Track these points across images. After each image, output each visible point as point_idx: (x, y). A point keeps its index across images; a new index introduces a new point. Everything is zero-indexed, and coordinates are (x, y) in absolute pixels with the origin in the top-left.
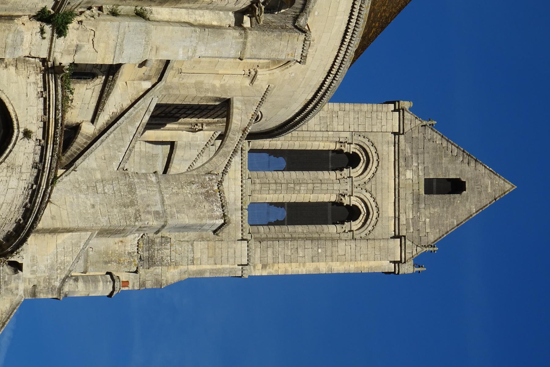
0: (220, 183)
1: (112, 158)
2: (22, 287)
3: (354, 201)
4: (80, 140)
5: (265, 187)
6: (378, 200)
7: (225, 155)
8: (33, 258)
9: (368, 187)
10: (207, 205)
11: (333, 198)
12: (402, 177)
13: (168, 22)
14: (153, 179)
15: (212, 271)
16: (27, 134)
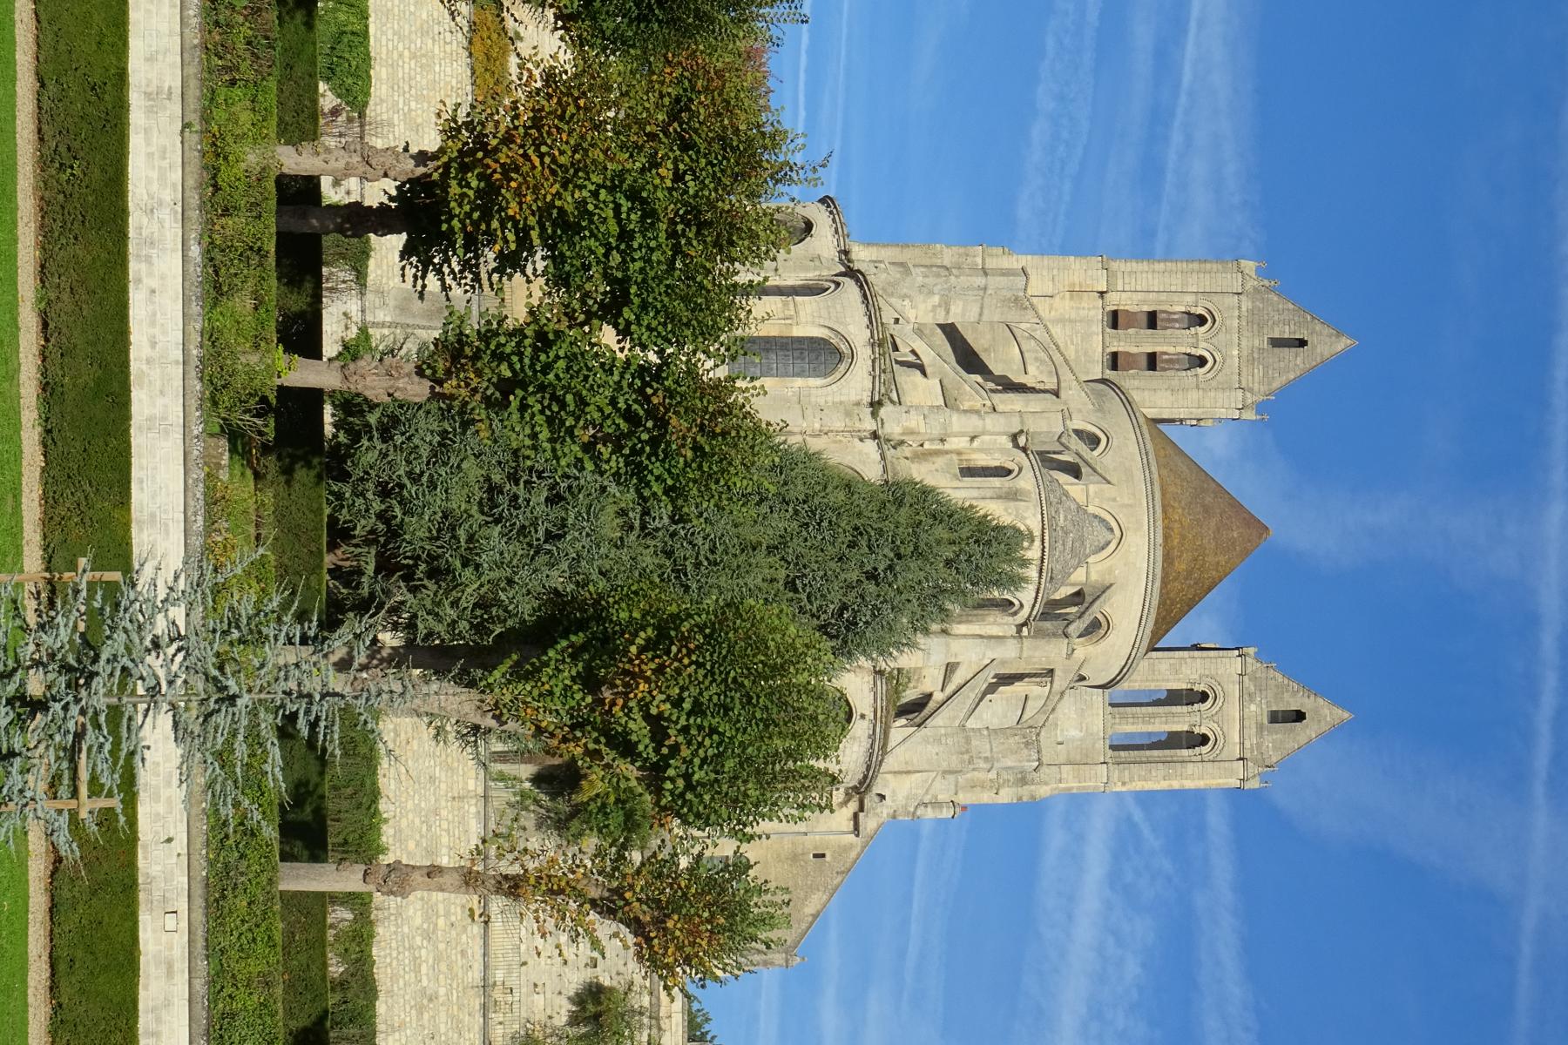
0: (1038, 735)
1: (955, 718)
2: (885, 812)
3: (1204, 730)
4: (931, 705)
5: (1124, 721)
6: (1225, 729)
7: (1045, 713)
8: (894, 791)
9: (1215, 718)
10: (1026, 751)
11: (1186, 728)
12: (1246, 710)
13: (965, 636)
14: (985, 732)
15: (1078, 788)
16: (863, 716)
